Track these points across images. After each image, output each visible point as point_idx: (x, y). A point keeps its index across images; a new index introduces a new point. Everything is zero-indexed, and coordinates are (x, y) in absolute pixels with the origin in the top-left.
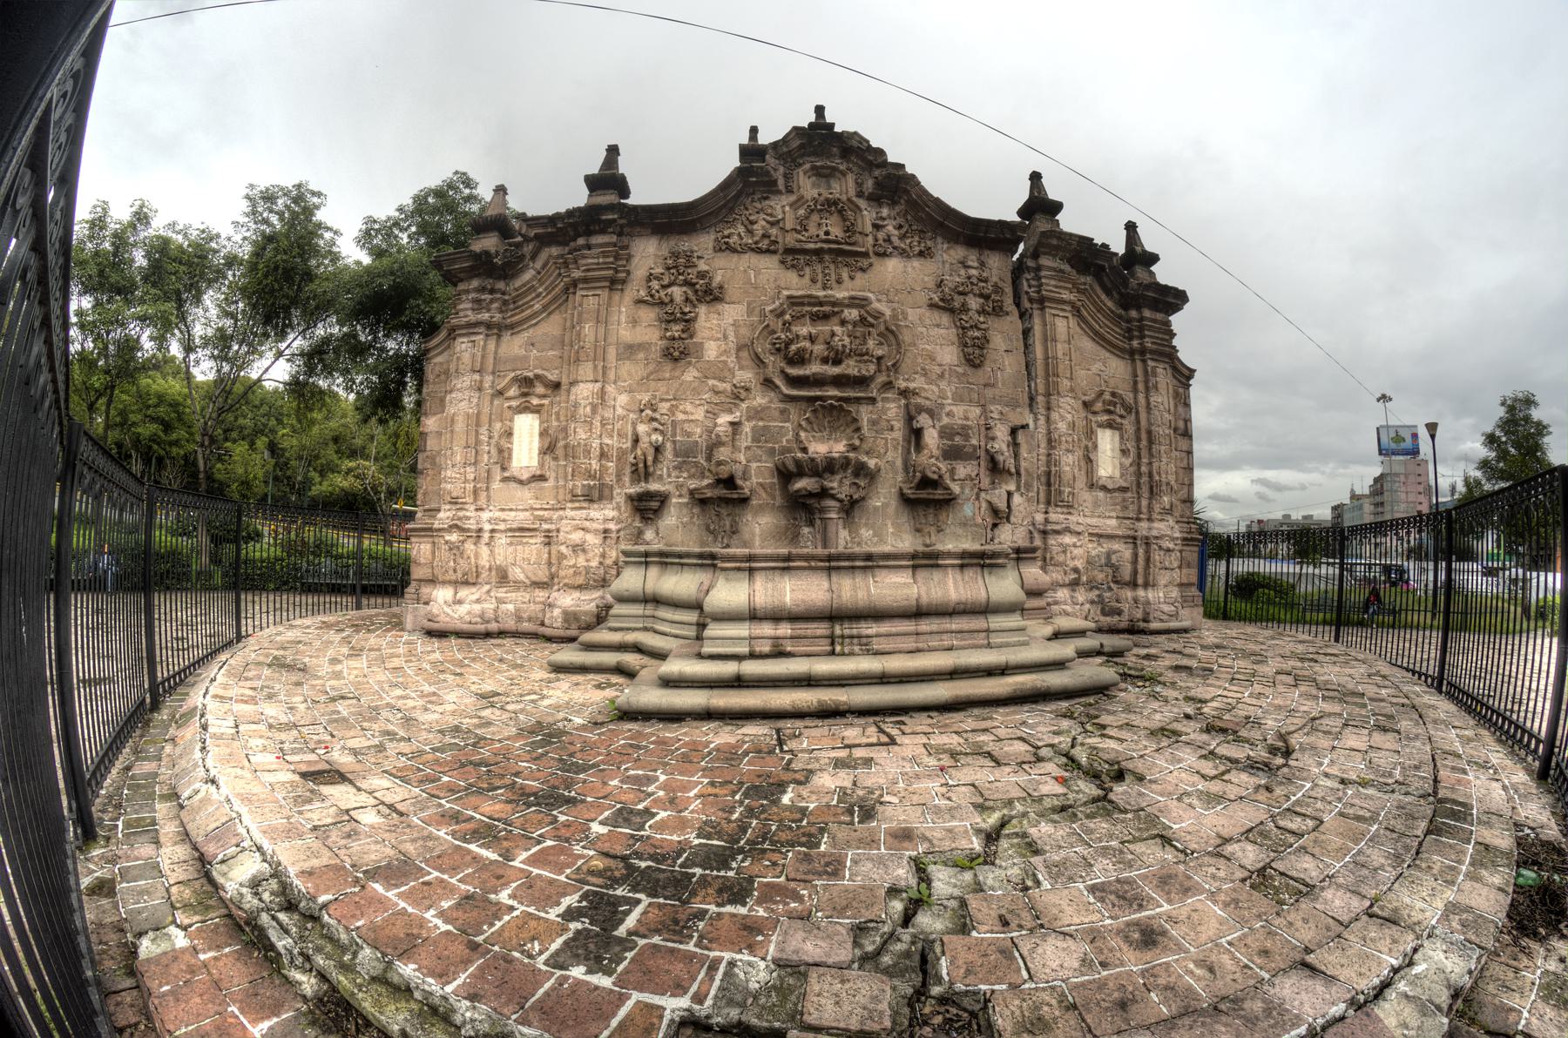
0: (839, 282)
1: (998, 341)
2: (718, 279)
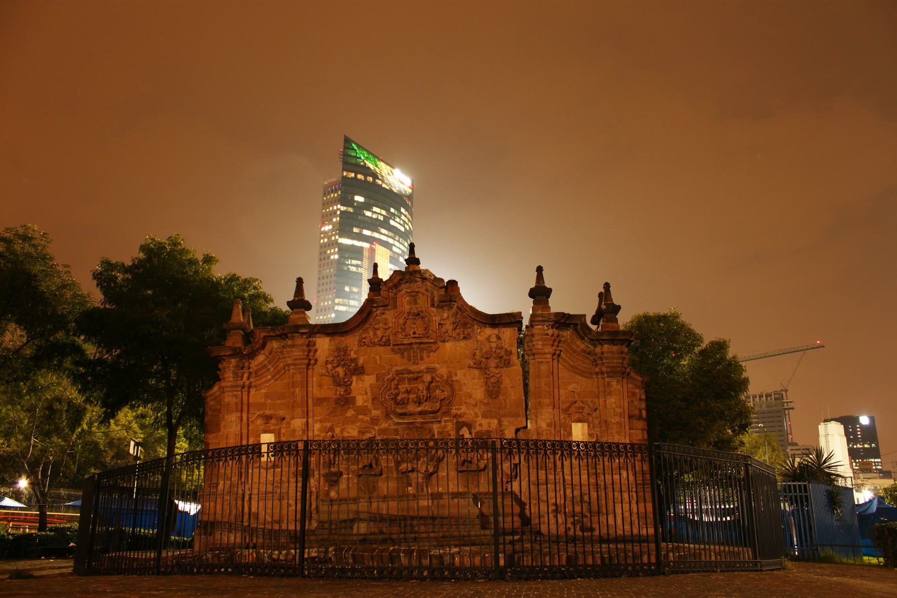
0: (422, 359)
1: (506, 382)
2: (361, 361)
